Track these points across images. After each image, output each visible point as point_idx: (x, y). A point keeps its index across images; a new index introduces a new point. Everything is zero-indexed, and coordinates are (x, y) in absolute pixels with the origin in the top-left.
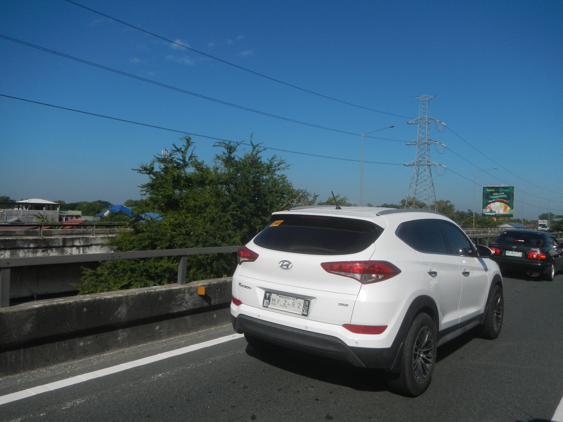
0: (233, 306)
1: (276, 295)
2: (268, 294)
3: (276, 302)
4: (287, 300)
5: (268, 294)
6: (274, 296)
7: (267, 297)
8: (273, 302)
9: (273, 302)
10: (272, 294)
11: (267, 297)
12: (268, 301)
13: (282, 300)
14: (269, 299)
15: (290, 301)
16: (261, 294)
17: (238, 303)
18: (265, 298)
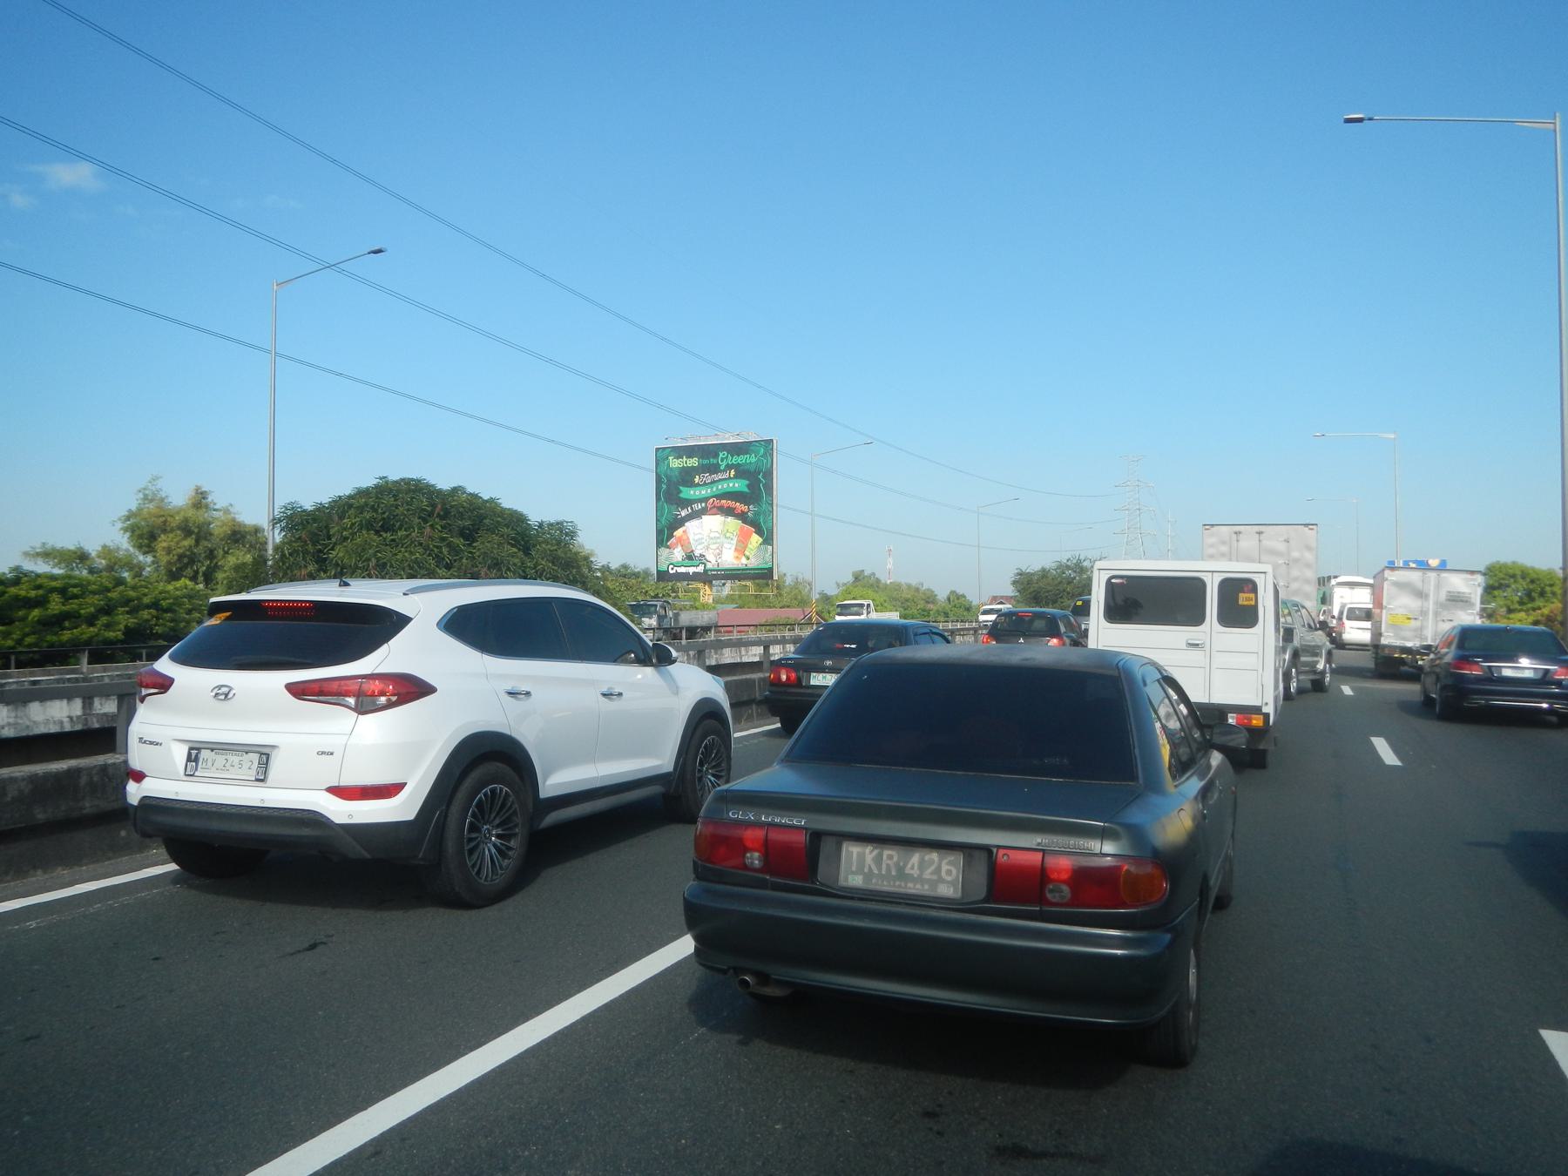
0: (132, 787)
1: (209, 751)
2: (194, 752)
3: (210, 763)
4: (228, 757)
5: (194, 752)
6: (205, 754)
7: (193, 757)
8: (204, 764)
9: (204, 764)
10: (203, 750)
11: (193, 757)
12: (194, 764)
13: (220, 759)
14: (196, 760)
15: (234, 759)
16: (180, 753)
17: (139, 777)
18: (189, 759)
